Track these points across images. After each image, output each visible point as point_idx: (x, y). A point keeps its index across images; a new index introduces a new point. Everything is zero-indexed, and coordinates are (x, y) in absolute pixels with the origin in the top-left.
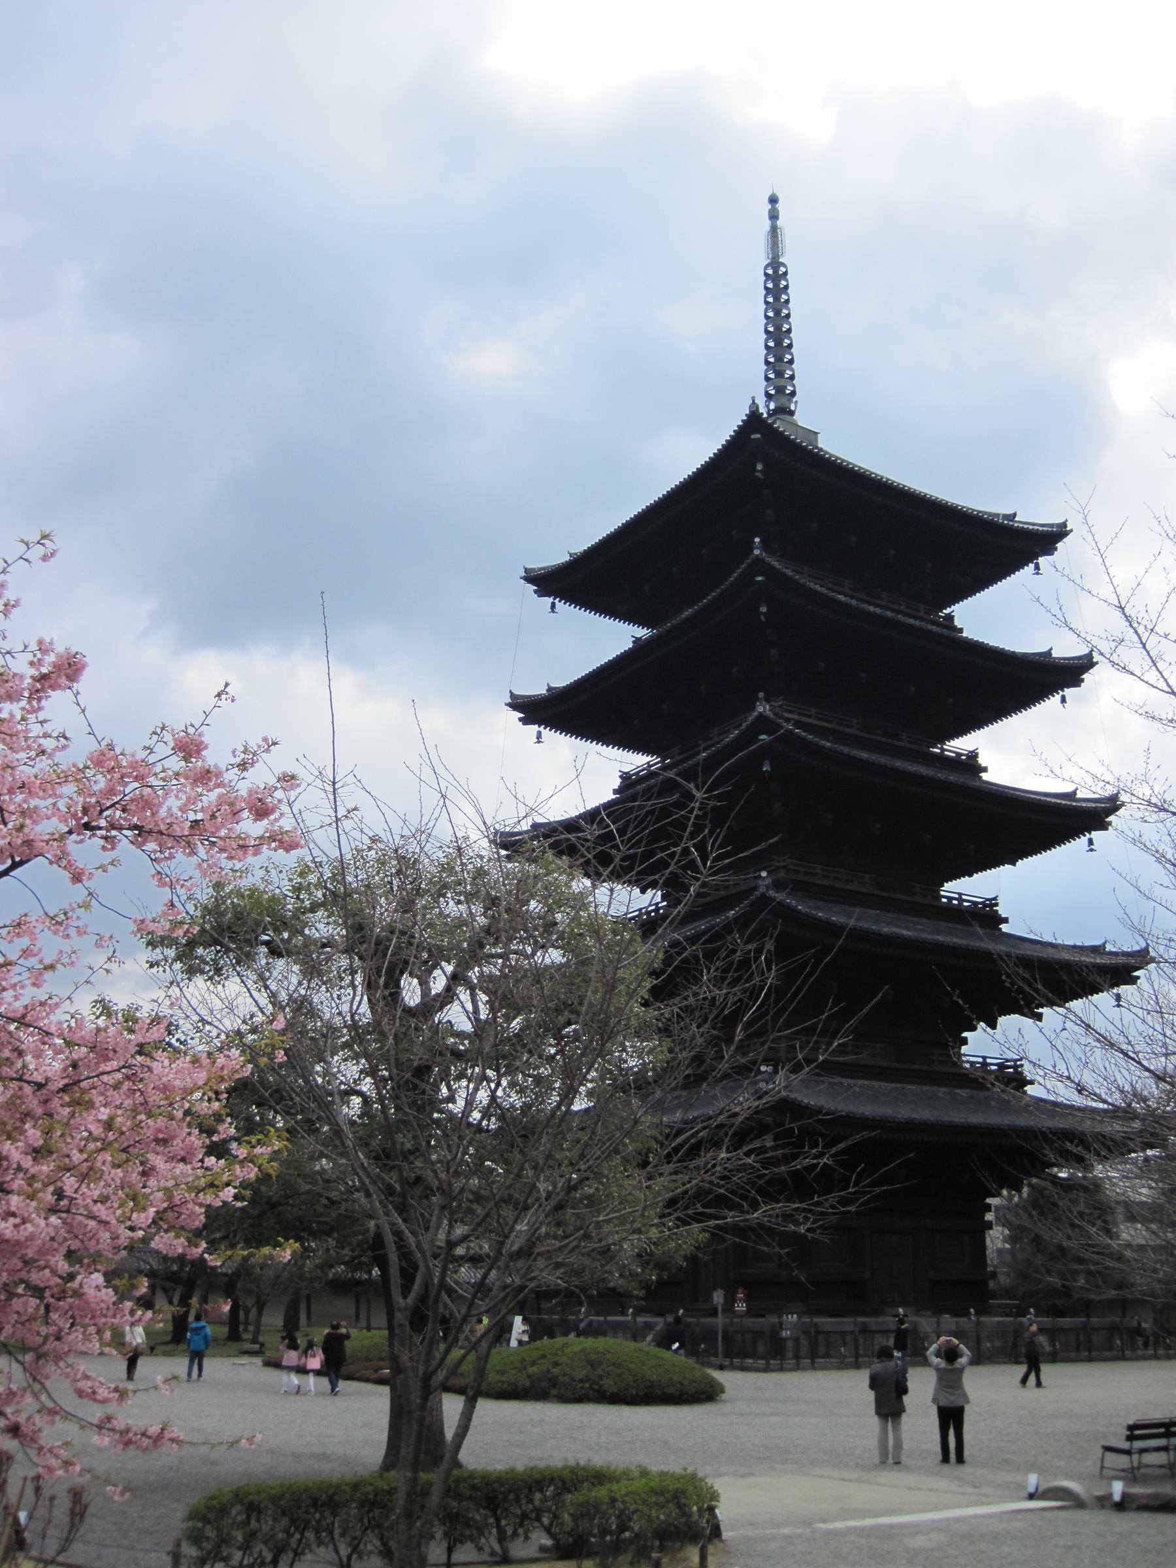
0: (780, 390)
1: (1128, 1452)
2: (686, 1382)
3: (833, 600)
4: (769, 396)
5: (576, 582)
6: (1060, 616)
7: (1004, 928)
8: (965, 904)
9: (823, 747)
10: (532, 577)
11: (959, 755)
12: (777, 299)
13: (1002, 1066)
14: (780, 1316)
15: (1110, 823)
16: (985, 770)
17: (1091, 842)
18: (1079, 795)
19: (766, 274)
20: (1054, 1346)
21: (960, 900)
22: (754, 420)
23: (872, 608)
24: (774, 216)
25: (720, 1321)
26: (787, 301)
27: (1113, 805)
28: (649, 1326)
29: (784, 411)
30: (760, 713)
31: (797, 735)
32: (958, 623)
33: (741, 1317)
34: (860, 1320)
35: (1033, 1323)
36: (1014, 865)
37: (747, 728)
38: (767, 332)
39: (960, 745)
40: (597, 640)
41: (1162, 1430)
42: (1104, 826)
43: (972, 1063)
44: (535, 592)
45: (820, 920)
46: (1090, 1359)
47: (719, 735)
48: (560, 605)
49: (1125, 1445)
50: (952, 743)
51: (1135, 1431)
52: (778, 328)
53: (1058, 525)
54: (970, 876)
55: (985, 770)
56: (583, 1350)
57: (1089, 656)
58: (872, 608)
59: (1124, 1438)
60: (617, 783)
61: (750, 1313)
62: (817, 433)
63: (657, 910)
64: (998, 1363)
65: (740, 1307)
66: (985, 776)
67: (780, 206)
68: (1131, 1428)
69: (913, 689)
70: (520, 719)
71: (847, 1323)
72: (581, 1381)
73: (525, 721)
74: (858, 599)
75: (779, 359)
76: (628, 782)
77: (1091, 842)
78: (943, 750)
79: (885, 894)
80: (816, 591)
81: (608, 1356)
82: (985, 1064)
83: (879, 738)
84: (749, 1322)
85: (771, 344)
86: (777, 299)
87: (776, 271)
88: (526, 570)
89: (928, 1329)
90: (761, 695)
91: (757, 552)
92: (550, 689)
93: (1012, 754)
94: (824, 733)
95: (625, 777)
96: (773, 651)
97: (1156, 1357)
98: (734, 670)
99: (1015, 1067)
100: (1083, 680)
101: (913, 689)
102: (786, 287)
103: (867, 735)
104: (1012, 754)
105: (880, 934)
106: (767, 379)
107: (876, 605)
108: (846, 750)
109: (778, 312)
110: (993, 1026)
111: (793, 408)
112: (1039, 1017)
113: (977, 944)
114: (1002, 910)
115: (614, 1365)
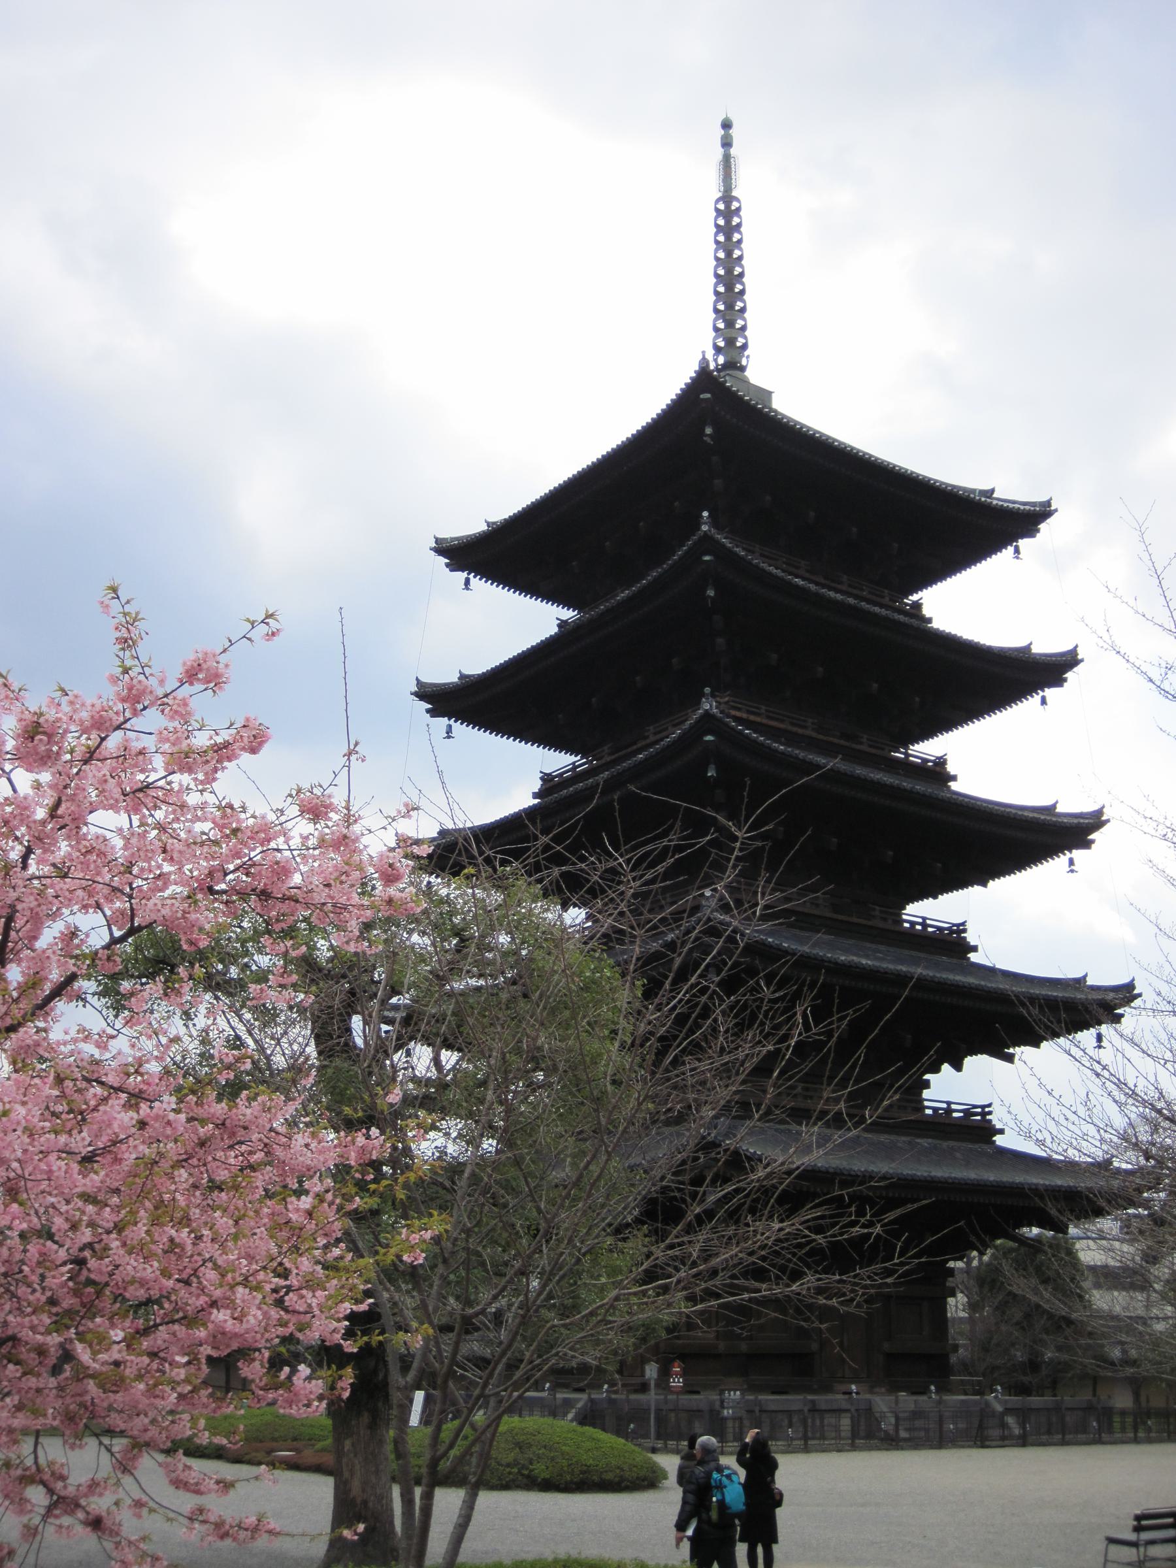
0: (730, 342)
1: (1134, 1544)
2: (626, 1467)
3: (789, 583)
4: (718, 350)
5: (497, 554)
6: (1106, 637)
7: (973, 957)
8: (930, 929)
9: (776, 750)
11: (925, 761)
12: (728, 238)
13: (968, 1113)
14: (722, 1392)
15: (1093, 841)
16: (954, 778)
17: (1071, 862)
18: (1060, 809)
19: (717, 210)
20: (1024, 1428)
21: (924, 925)
22: (704, 380)
23: (832, 594)
24: (727, 143)
25: (652, 1398)
26: (740, 241)
27: (1095, 821)
28: (568, 1404)
29: (734, 366)
30: (707, 714)
31: (747, 736)
32: (927, 611)
33: (678, 1393)
34: (810, 1397)
35: (997, 1399)
36: (985, 885)
37: (692, 727)
38: (717, 276)
39: (927, 749)
41: (1170, 1520)
42: (1087, 844)
43: (935, 1110)
44: (447, 565)
45: (770, 946)
46: (1064, 1443)
47: (655, 734)
48: (475, 581)
49: (1133, 1537)
50: (917, 747)
51: (1142, 1522)
52: (729, 271)
53: (1042, 504)
54: (935, 897)
55: (954, 778)
56: (511, 1431)
57: (1073, 652)
58: (832, 594)
59: (1131, 1528)
60: (537, 785)
61: (689, 1390)
62: (770, 393)
64: (963, 1447)
65: (677, 1382)
66: (953, 786)
67: (733, 132)
68: (1138, 1518)
69: (875, 686)
70: (428, 711)
71: (795, 1401)
72: (508, 1465)
73: (434, 713)
74: (817, 584)
75: (730, 306)
76: (550, 785)
77: (1071, 862)
78: (907, 755)
79: (840, 917)
80: (770, 574)
81: (539, 1437)
82: (949, 1111)
83: (836, 741)
84: (687, 1400)
85: (721, 289)
86: (728, 238)
87: (728, 206)
88: (437, 540)
89: (885, 1410)
90: (707, 690)
91: (705, 528)
92: (462, 676)
93: (984, 758)
94: (775, 734)
95: (547, 778)
96: (720, 641)
97: (1136, 1441)
98: (675, 661)
99: (984, 1114)
100: (1065, 680)
101: (875, 686)
102: (739, 225)
103: (821, 737)
104: (984, 758)
105: (836, 963)
106: (716, 329)
107: (837, 591)
108: (802, 755)
109: (729, 254)
110: (958, 1067)
111: (744, 362)
112: (1010, 1058)
113: (944, 976)
114: (971, 937)
115: (545, 1447)
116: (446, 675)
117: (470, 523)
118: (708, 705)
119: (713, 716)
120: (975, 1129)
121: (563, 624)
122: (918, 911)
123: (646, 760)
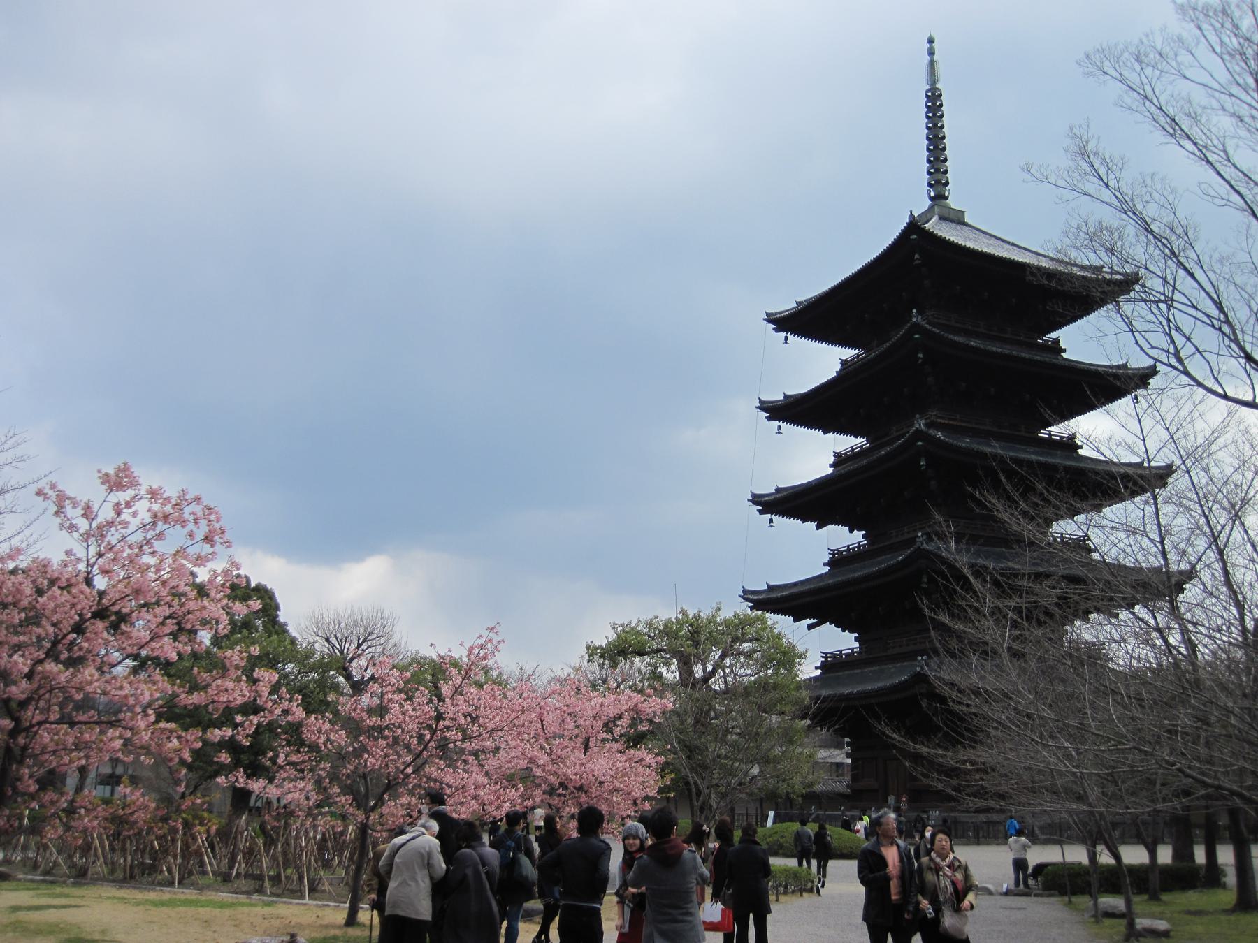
4: (930, 185)
10: (771, 319)
12: (934, 115)
21: (1062, 537)
29: (939, 197)
32: (1062, 345)
48: (791, 337)
52: (936, 136)
60: (832, 460)
61: (910, 809)
63: (859, 546)
66: (1080, 451)
67: (935, 45)
73: (769, 419)
75: (937, 159)
78: (1050, 435)
86: (934, 115)
87: (933, 94)
92: (786, 397)
93: (1099, 432)
94: (963, 431)
95: (837, 455)
104: (1099, 432)
106: (929, 173)
109: (935, 125)
116: (776, 396)
118: (920, 424)
119: (922, 431)
120: (1094, 656)
121: (844, 362)
123: (887, 454)
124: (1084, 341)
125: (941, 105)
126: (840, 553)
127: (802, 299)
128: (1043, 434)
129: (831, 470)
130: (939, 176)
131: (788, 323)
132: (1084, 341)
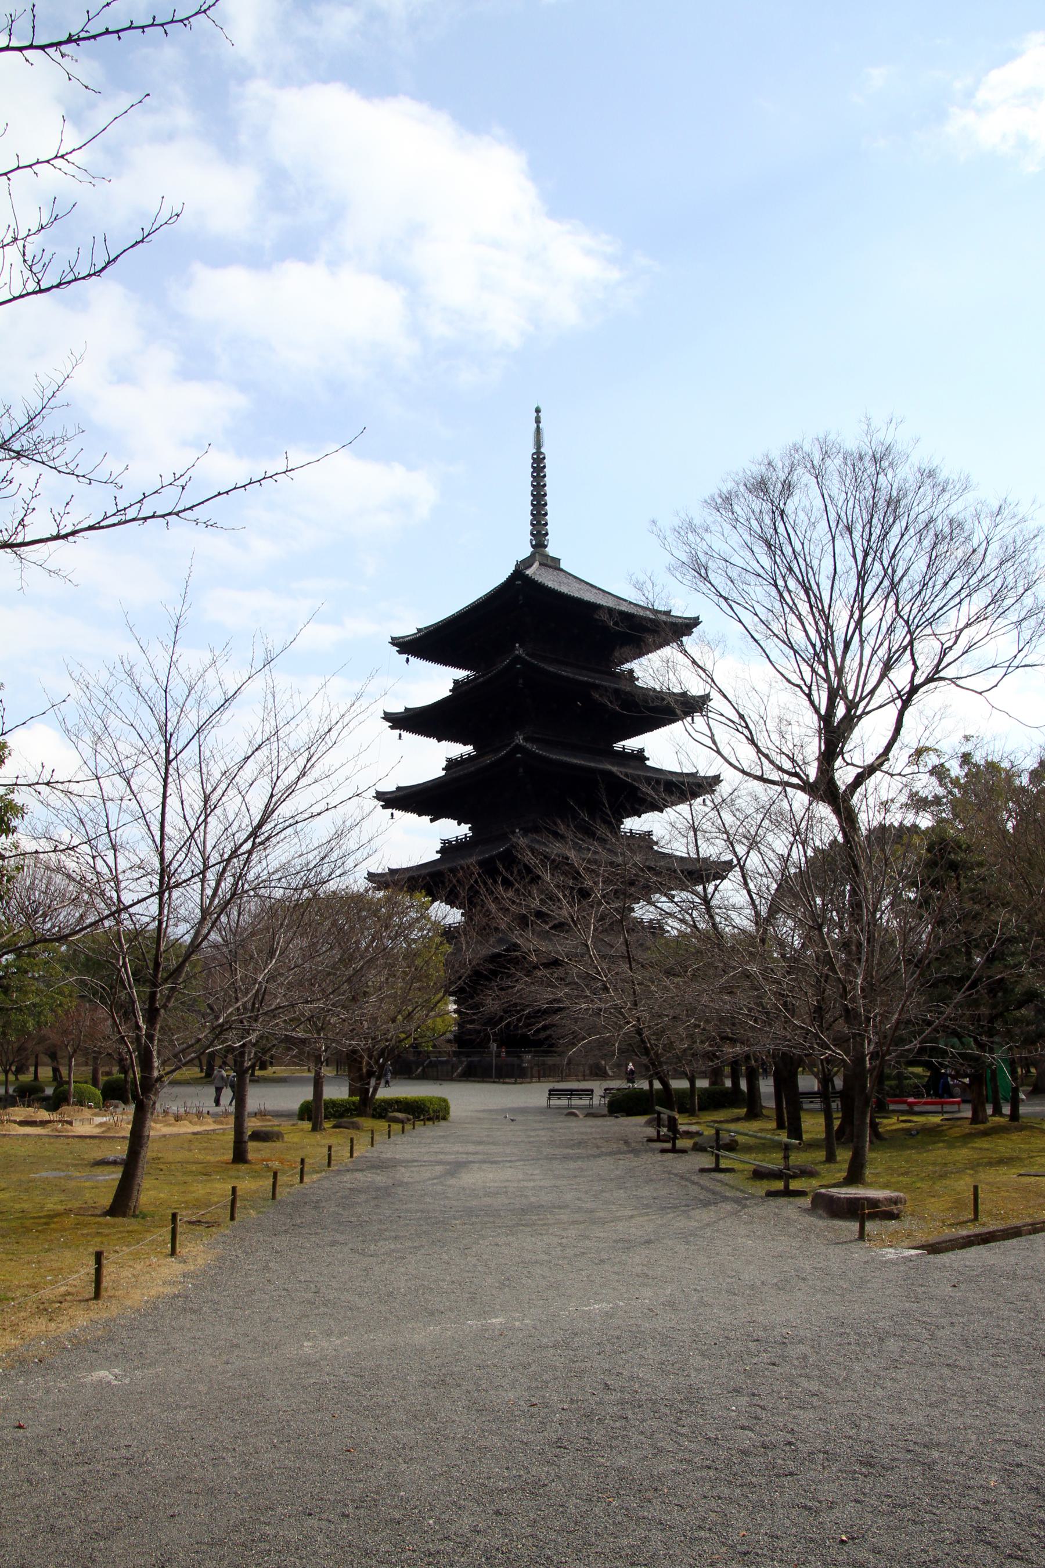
19: (533, 459)
22: (518, 574)
24: (538, 421)
39: (632, 744)
40: (435, 682)
48: (412, 659)
60: (444, 764)
63: (466, 837)
66: (648, 763)
73: (392, 728)
76: (452, 765)
78: (624, 748)
86: (538, 475)
88: (392, 638)
92: (406, 709)
93: (663, 748)
109: (538, 484)
117: (408, 629)
121: (456, 682)
122: (632, 824)
124: (653, 670)
125: (544, 467)
126: (450, 842)
127: (422, 625)
128: (618, 746)
129: (443, 773)
130: (538, 528)
131: (409, 646)
132: (653, 670)
